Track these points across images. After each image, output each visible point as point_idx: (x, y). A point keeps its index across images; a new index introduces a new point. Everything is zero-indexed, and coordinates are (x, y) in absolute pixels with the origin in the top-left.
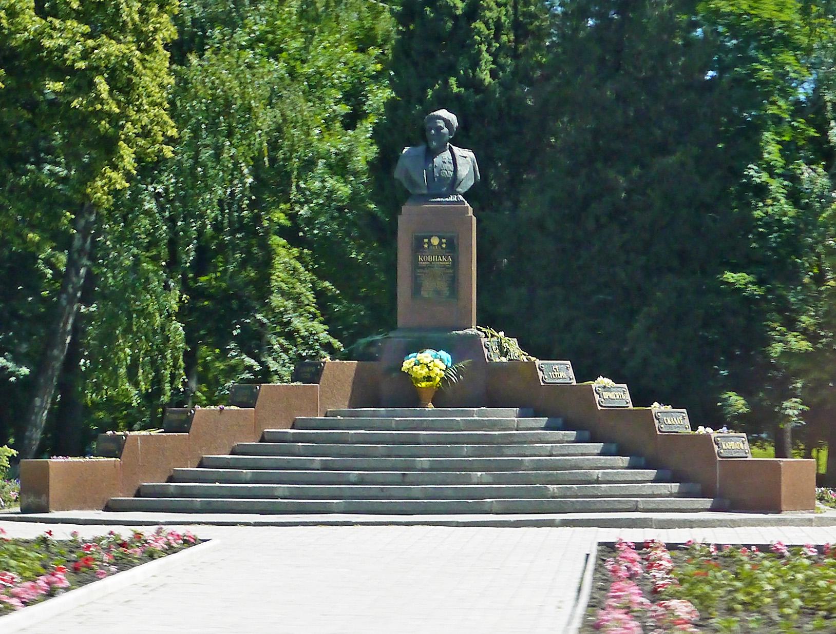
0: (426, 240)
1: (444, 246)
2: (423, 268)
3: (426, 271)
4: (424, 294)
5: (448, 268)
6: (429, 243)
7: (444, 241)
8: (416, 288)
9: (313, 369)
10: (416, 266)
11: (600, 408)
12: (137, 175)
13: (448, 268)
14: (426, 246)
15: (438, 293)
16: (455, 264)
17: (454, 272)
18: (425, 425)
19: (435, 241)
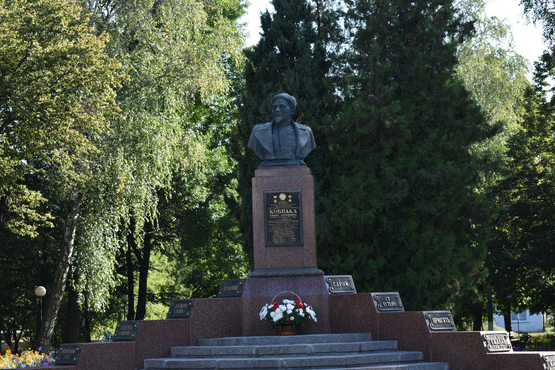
0: (275, 197)
1: (290, 201)
2: (273, 219)
3: (276, 222)
4: (275, 241)
5: (294, 219)
6: (278, 199)
7: (290, 197)
8: (269, 236)
9: (186, 305)
10: (267, 217)
11: (378, 312)
12: (321, 51)
13: (294, 219)
14: (275, 201)
15: (287, 239)
16: (299, 215)
17: (299, 222)
18: (281, 351)
19: (283, 197)
